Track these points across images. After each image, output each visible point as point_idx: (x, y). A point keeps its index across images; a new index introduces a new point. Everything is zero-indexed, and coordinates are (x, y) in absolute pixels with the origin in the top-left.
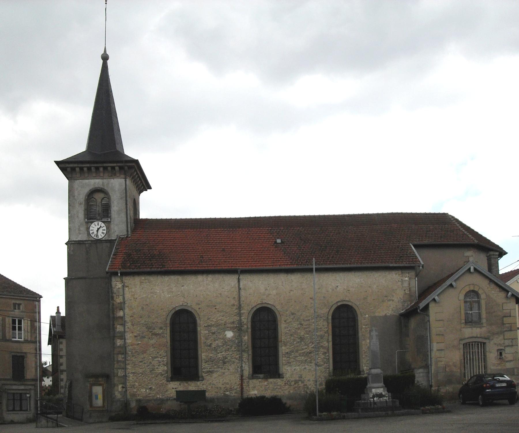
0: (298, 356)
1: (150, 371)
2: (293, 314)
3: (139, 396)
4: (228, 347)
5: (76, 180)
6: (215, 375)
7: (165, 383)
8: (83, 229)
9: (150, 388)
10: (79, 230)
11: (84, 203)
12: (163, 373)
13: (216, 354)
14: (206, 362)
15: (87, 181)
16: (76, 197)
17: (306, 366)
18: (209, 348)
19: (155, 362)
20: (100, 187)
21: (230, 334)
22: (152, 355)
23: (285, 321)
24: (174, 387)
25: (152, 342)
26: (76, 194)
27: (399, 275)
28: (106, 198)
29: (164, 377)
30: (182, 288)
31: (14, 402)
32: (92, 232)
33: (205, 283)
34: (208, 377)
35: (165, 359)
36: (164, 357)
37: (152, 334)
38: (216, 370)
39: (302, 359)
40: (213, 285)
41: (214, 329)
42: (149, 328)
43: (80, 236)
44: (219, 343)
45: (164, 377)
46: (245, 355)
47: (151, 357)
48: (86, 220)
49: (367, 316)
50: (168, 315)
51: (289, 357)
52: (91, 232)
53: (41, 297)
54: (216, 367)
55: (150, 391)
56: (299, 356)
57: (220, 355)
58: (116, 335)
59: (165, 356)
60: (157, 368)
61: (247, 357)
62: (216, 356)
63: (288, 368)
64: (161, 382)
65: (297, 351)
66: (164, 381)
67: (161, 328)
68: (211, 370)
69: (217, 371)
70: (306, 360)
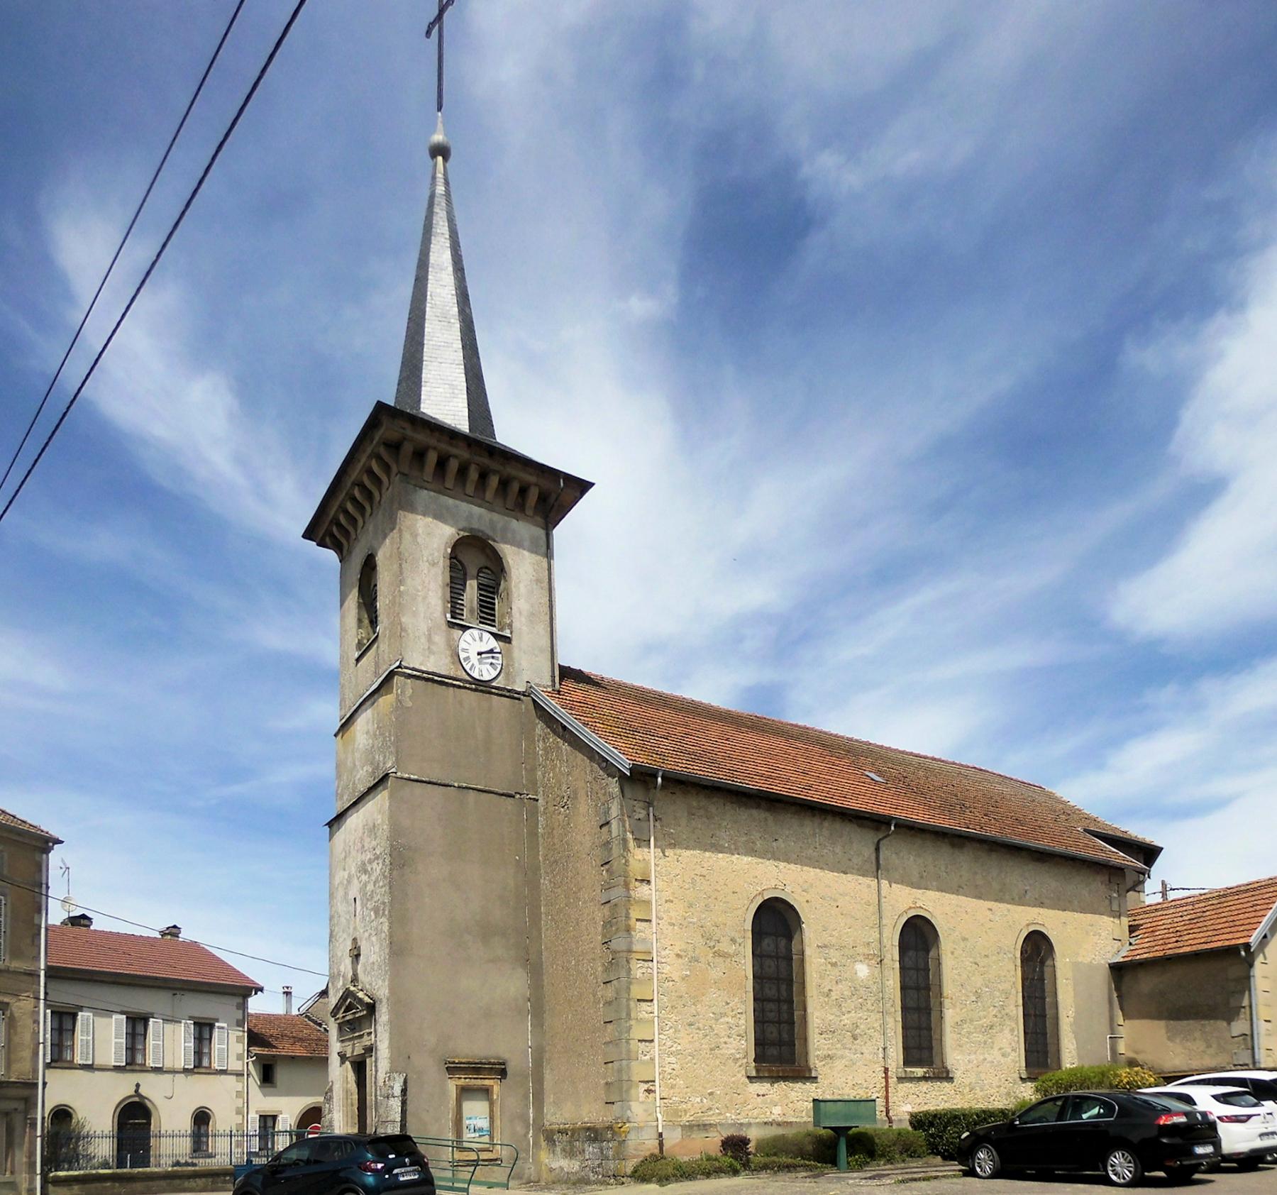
0: (973, 1033)
1: (711, 1050)
2: (964, 939)
3: (686, 1115)
4: (860, 1000)
5: (421, 488)
6: (839, 1064)
7: (741, 1081)
8: (439, 639)
9: (711, 1094)
10: (429, 639)
11: (441, 564)
12: (738, 1056)
13: (839, 1016)
14: (821, 1034)
15: (451, 501)
16: (419, 540)
17: (986, 1056)
18: (826, 1000)
19: (720, 1028)
20: (482, 532)
21: (863, 970)
22: (714, 1009)
23: (952, 953)
24: (761, 1093)
25: (715, 974)
26: (420, 531)
27: (1106, 885)
28: (487, 571)
29: (740, 1066)
30: (774, 844)
31: (776, 1022)
32: (466, 655)
33: (817, 839)
34: (826, 1070)
35: (742, 1022)
36: (739, 1016)
37: (714, 953)
38: (839, 1053)
39: (979, 1039)
40: (831, 849)
41: (835, 956)
42: (707, 937)
43: (432, 658)
44: (844, 988)
45: (740, 1066)
46: (890, 1020)
47: (713, 1013)
48: (449, 616)
49: (1068, 960)
50: (747, 909)
51: (960, 1034)
52: (462, 655)
53: (45, 843)
54: (839, 1046)
55: (711, 1100)
56: (975, 1032)
57: (846, 1020)
58: (635, 948)
59: (742, 1013)
60: (725, 1043)
61: (893, 1028)
62: (841, 1021)
63: (959, 1058)
64: (733, 1079)
65: (971, 1021)
66: (740, 1075)
67: (733, 940)
68: (830, 1053)
69: (842, 1057)
70: (985, 1043)
